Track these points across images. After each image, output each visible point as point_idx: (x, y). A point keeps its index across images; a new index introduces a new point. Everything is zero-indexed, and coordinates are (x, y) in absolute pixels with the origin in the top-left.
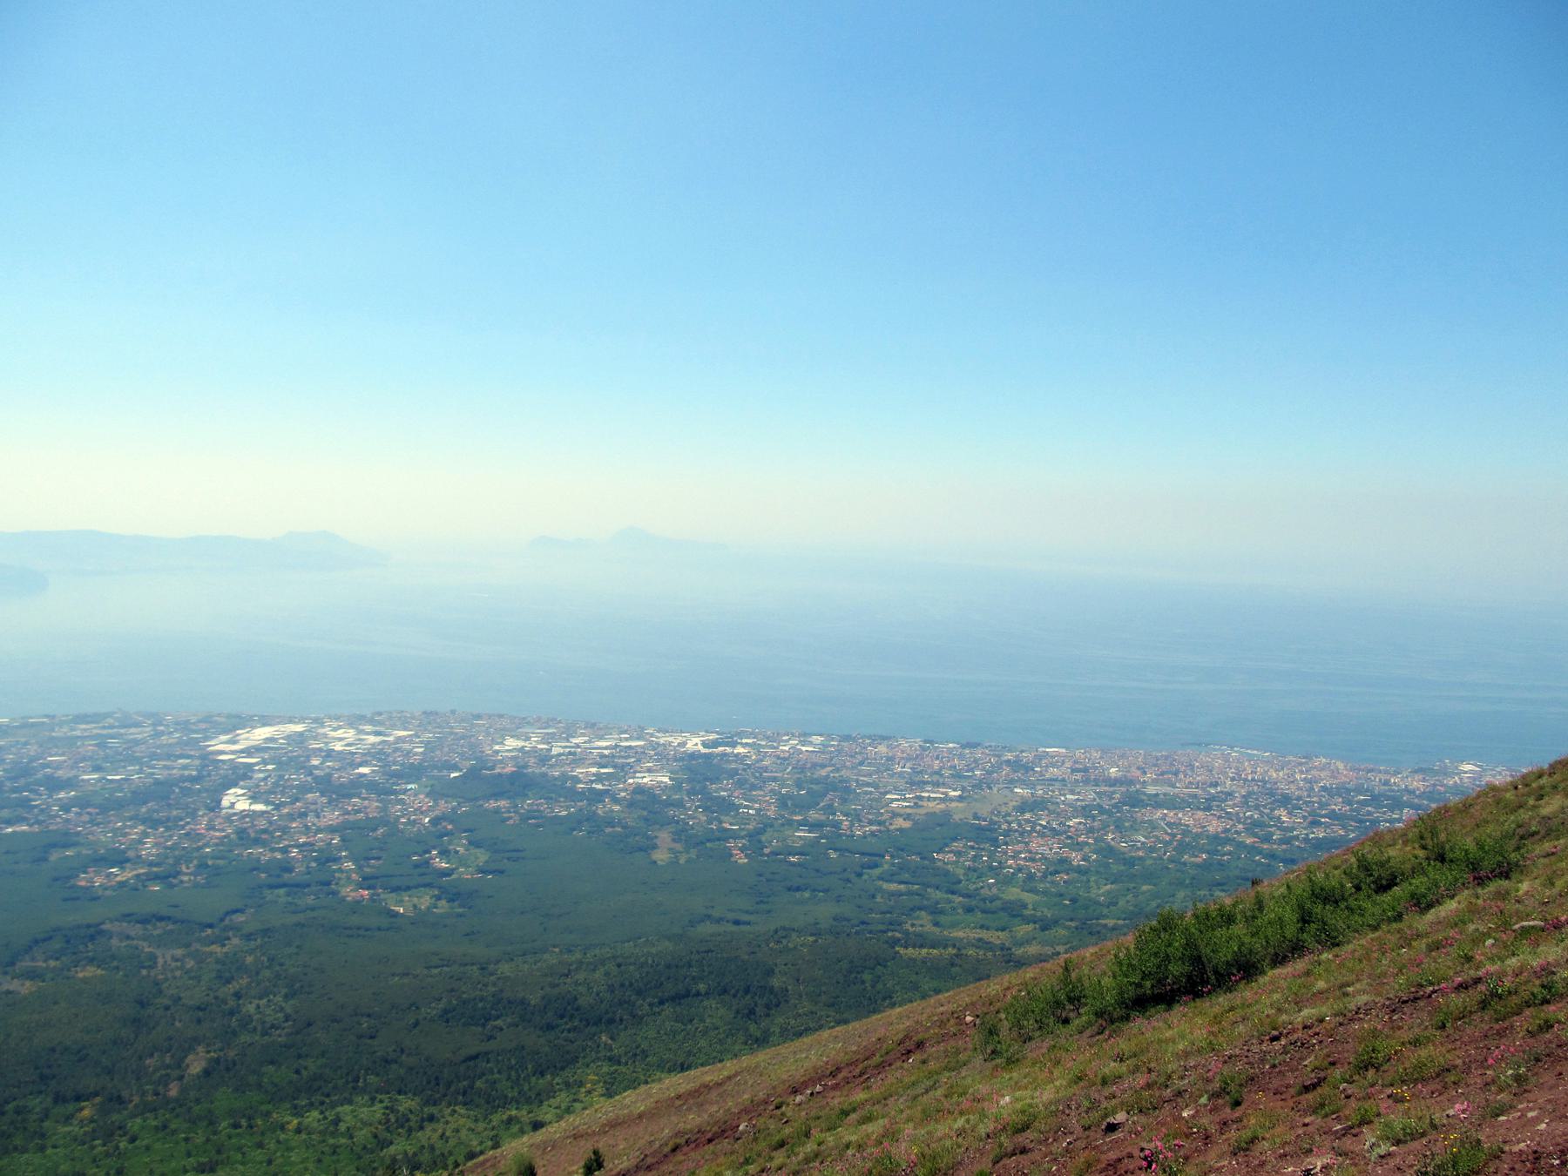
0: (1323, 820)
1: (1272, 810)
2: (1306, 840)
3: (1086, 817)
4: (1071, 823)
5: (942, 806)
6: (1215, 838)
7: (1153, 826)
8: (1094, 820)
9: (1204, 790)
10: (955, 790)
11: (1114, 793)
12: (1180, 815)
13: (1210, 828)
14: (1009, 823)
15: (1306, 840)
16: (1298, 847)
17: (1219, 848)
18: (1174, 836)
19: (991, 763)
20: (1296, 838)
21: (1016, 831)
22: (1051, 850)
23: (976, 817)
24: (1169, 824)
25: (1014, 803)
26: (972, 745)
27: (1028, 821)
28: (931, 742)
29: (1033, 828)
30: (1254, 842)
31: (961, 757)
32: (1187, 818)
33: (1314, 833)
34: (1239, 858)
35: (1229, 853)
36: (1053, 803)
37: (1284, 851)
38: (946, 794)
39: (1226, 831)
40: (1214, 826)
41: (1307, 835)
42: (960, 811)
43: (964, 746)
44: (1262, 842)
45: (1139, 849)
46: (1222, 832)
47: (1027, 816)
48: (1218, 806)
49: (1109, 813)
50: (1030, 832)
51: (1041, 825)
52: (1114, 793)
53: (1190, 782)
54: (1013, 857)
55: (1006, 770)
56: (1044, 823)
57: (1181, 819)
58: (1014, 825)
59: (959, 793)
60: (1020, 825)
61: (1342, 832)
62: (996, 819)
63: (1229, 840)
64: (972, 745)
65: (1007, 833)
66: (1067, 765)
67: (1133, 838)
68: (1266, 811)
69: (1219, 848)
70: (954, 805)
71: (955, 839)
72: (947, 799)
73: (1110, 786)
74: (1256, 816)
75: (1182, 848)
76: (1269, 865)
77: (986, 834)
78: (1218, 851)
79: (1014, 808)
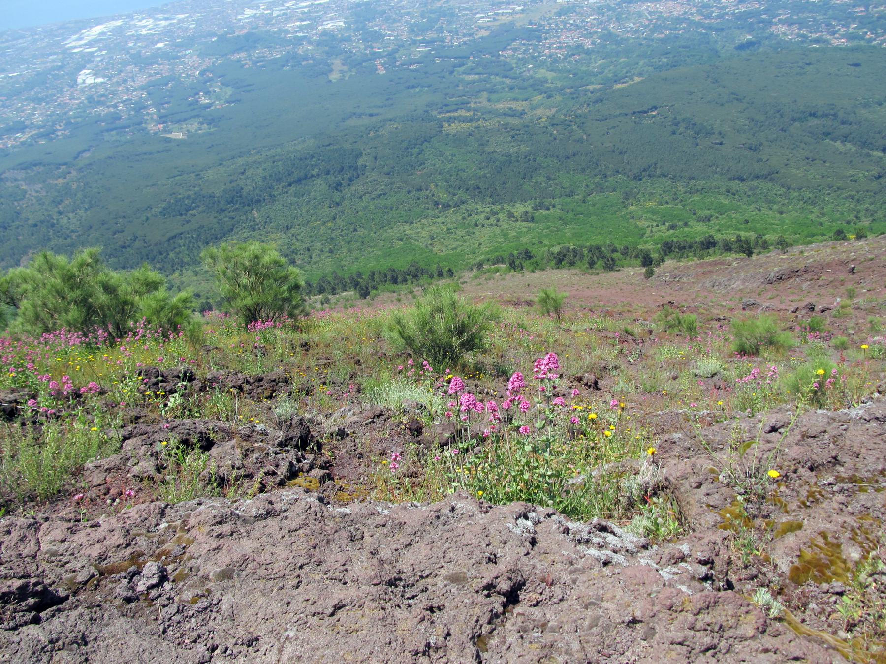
2: (734, 14)
3: (599, 14)
4: (588, 20)
5: (510, 18)
6: (678, 20)
7: (640, 15)
8: (603, 16)
10: (519, 6)
12: (658, 6)
13: (675, 13)
14: (550, 24)
15: (734, 14)
16: (728, 19)
18: (651, 20)
20: (727, 14)
21: (554, 29)
22: (573, 39)
23: (530, 23)
25: (555, 10)
27: (562, 21)
29: (564, 27)
30: (701, 19)
33: (738, 9)
34: (689, 31)
35: (684, 29)
36: (579, 7)
37: (718, 23)
39: (685, 13)
41: (734, 11)
42: (521, 21)
44: (705, 19)
45: (628, 32)
46: (682, 14)
47: (563, 17)
49: (614, 10)
50: (562, 29)
51: (569, 23)
54: (551, 48)
56: (571, 22)
57: (657, 9)
58: (553, 26)
59: (522, 7)
60: (557, 25)
62: (542, 22)
63: (686, 19)
70: (518, 16)
71: (514, 40)
72: (514, 13)
75: (656, 28)
76: (706, 34)
77: (534, 34)
78: (677, 28)
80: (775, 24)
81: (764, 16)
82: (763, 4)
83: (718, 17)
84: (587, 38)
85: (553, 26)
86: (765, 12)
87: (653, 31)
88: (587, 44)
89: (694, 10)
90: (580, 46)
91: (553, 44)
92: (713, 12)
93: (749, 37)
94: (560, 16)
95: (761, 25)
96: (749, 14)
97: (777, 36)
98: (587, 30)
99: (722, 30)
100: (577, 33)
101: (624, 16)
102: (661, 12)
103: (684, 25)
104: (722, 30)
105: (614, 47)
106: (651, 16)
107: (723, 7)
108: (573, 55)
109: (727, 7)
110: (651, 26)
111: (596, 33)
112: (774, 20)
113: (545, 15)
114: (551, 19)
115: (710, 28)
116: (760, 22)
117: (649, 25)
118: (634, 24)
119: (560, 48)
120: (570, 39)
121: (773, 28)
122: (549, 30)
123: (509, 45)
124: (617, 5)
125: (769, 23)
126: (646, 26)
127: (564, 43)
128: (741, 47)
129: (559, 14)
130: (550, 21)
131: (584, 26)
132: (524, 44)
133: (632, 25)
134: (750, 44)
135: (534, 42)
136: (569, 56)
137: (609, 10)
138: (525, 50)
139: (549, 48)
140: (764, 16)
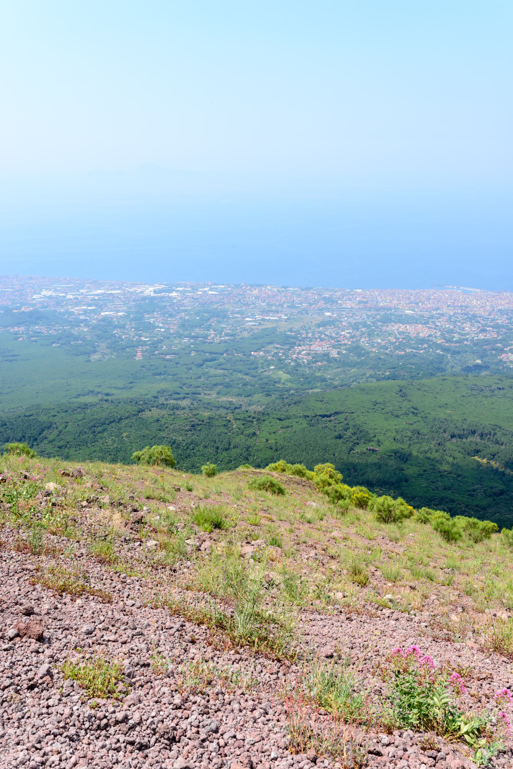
0: (488, 329)
1: (462, 323)
2: (472, 340)
3: (354, 329)
5: (275, 325)
6: (423, 341)
8: (358, 331)
9: (430, 312)
11: (376, 315)
12: (408, 327)
13: (421, 335)
14: (307, 333)
15: (472, 340)
17: (420, 346)
18: (398, 339)
19: (315, 298)
20: (467, 340)
21: (310, 338)
24: (400, 333)
25: (317, 322)
26: (308, 289)
27: (319, 332)
28: (285, 287)
30: (442, 342)
31: (299, 296)
32: (411, 329)
34: (429, 351)
35: (425, 348)
36: (339, 321)
38: (280, 317)
39: (430, 336)
40: (424, 332)
41: (473, 338)
43: (303, 290)
44: (447, 342)
46: (428, 337)
47: (321, 329)
48: (433, 322)
50: (316, 338)
51: (325, 334)
52: (376, 315)
53: (423, 308)
55: (321, 304)
56: (327, 333)
57: (407, 330)
60: (313, 334)
61: (496, 336)
64: (308, 289)
65: (303, 339)
66: (358, 299)
67: (375, 341)
68: (459, 324)
69: (420, 346)
71: (271, 343)
73: (377, 311)
74: (451, 327)
76: (443, 355)
78: (418, 347)
79: (316, 324)
80: (506, 352)
81: (499, 345)
82: (501, 335)
83: (456, 342)
84: (336, 349)
85: (310, 335)
86: (500, 341)
87: (397, 348)
88: (334, 354)
89: (439, 334)
90: (326, 355)
91: (303, 350)
92: (454, 337)
93: (479, 361)
94: (319, 327)
95: (494, 352)
96: (486, 342)
97: (505, 362)
98: (339, 341)
99: (459, 353)
100: (328, 343)
101: (376, 333)
102: (409, 333)
103: (426, 346)
104: (459, 353)
105: (356, 358)
106: (400, 335)
107: (465, 334)
108: (316, 361)
109: (469, 334)
110: (397, 343)
111: (345, 345)
112: (505, 349)
113: (306, 325)
114: (310, 329)
115: (446, 350)
116: (493, 350)
117: (396, 342)
118: (382, 340)
119: (308, 354)
120: (318, 348)
121: (504, 355)
122: (305, 338)
123: (264, 347)
124: (373, 323)
125: (502, 351)
126: (392, 343)
127: (313, 351)
128: (468, 369)
129: (319, 326)
130: (309, 331)
131: (337, 338)
132: (277, 348)
133: (379, 341)
134: (478, 367)
135: (287, 347)
136: (313, 362)
137: (364, 327)
138: (276, 353)
139: (299, 353)
140: (499, 345)
